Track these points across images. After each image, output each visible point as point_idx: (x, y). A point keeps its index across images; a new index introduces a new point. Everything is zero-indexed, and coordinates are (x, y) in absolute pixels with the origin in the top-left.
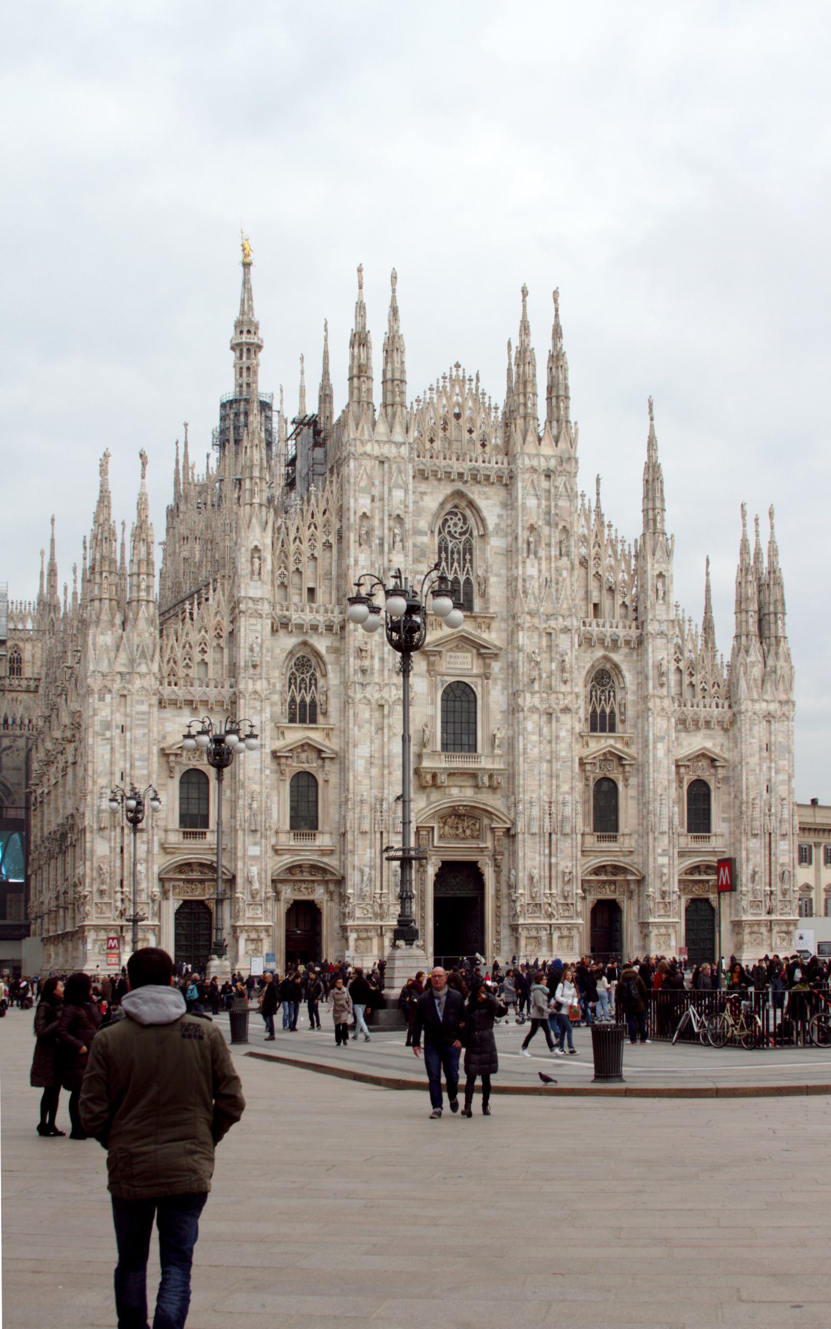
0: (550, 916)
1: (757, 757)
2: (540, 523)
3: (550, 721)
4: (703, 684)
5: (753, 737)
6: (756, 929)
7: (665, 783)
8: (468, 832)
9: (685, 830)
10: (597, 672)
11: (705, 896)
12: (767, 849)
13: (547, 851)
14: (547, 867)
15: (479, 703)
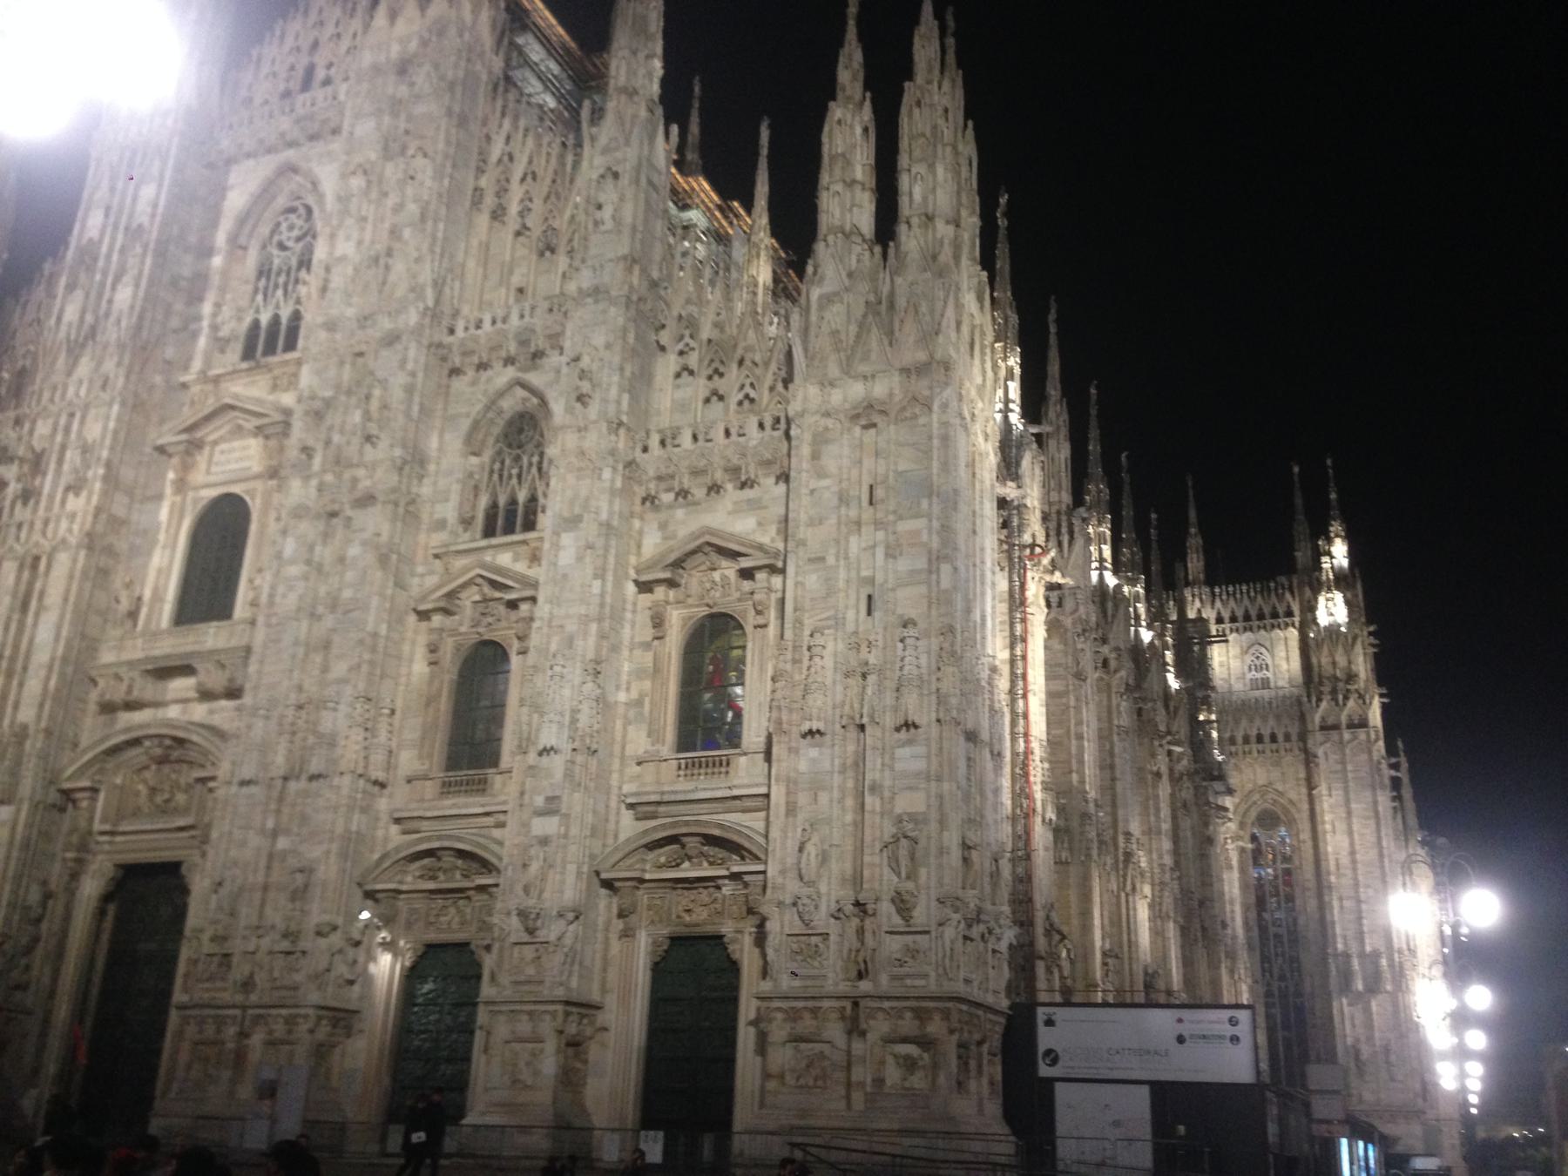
2: (373, 156)
4: (748, 389)
5: (821, 474)
6: (807, 1024)
9: (667, 748)
10: (510, 423)
11: (709, 929)
13: (270, 824)
14: (263, 863)
15: (254, 527)
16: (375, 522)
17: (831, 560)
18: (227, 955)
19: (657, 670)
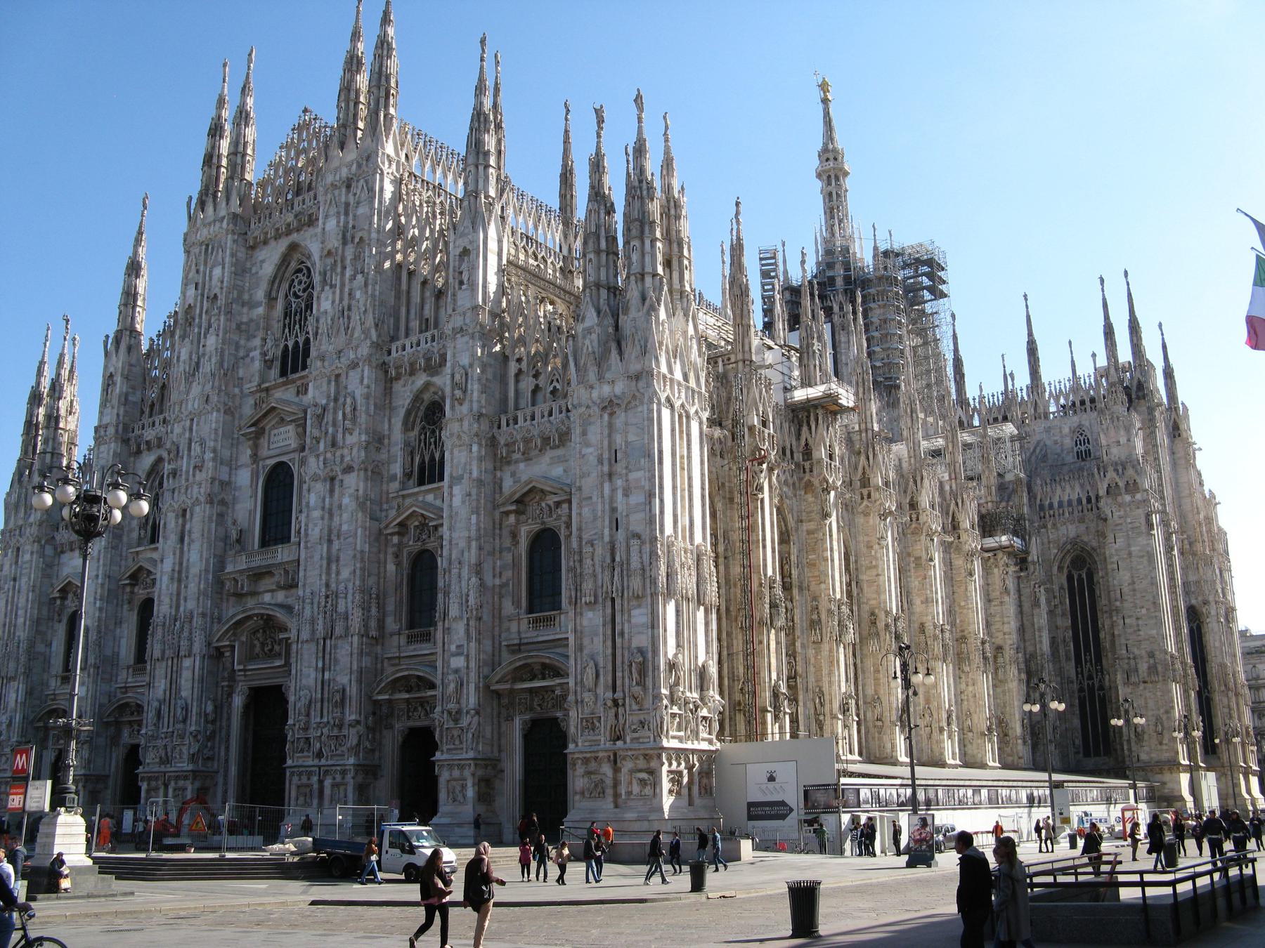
0: (319, 755)
1: (594, 474)
3: (332, 491)
5: (588, 445)
6: (593, 766)
7: (462, 544)
8: (277, 648)
10: (428, 408)
11: (550, 715)
12: (609, 627)
13: (320, 665)
16: (353, 482)
17: (595, 499)
18: (307, 739)
19: (515, 565)
